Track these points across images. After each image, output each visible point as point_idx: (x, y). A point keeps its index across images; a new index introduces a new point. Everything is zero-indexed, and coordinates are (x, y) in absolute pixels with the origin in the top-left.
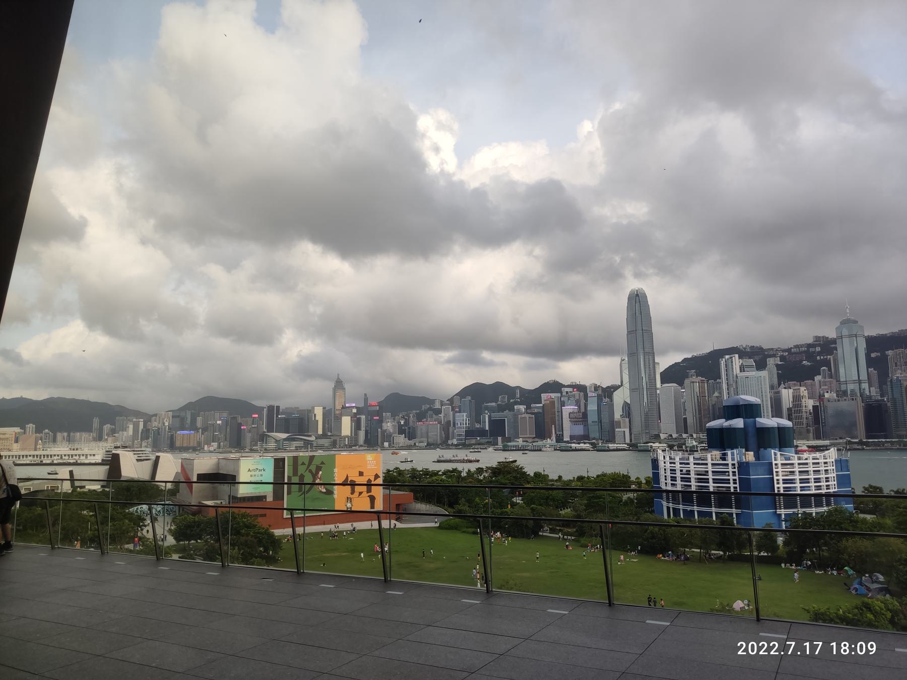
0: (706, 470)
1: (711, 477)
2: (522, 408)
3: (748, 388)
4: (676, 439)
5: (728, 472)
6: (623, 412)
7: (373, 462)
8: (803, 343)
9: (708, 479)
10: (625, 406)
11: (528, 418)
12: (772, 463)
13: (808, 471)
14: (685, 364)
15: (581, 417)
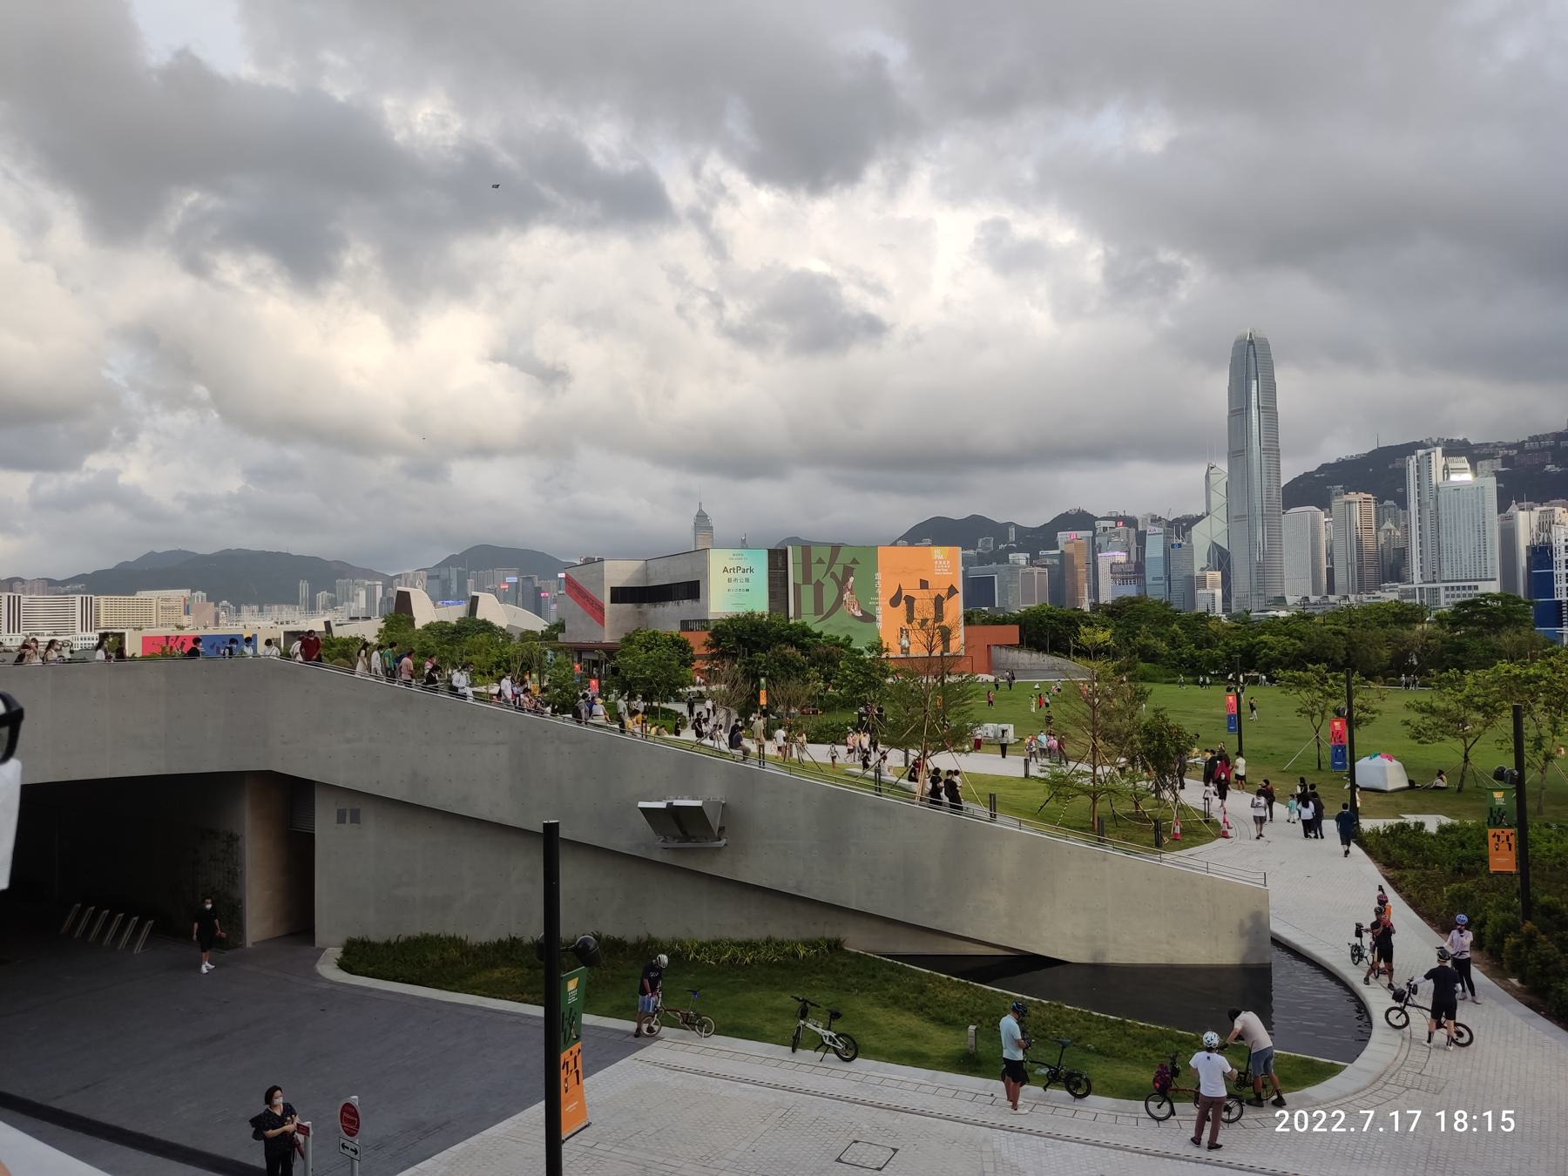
2: (1021, 558)
4: (1315, 604)
6: (1209, 561)
10: (1214, 553)
11: (1036, 575)
14: (1323, 475)
15: (1133, 570)
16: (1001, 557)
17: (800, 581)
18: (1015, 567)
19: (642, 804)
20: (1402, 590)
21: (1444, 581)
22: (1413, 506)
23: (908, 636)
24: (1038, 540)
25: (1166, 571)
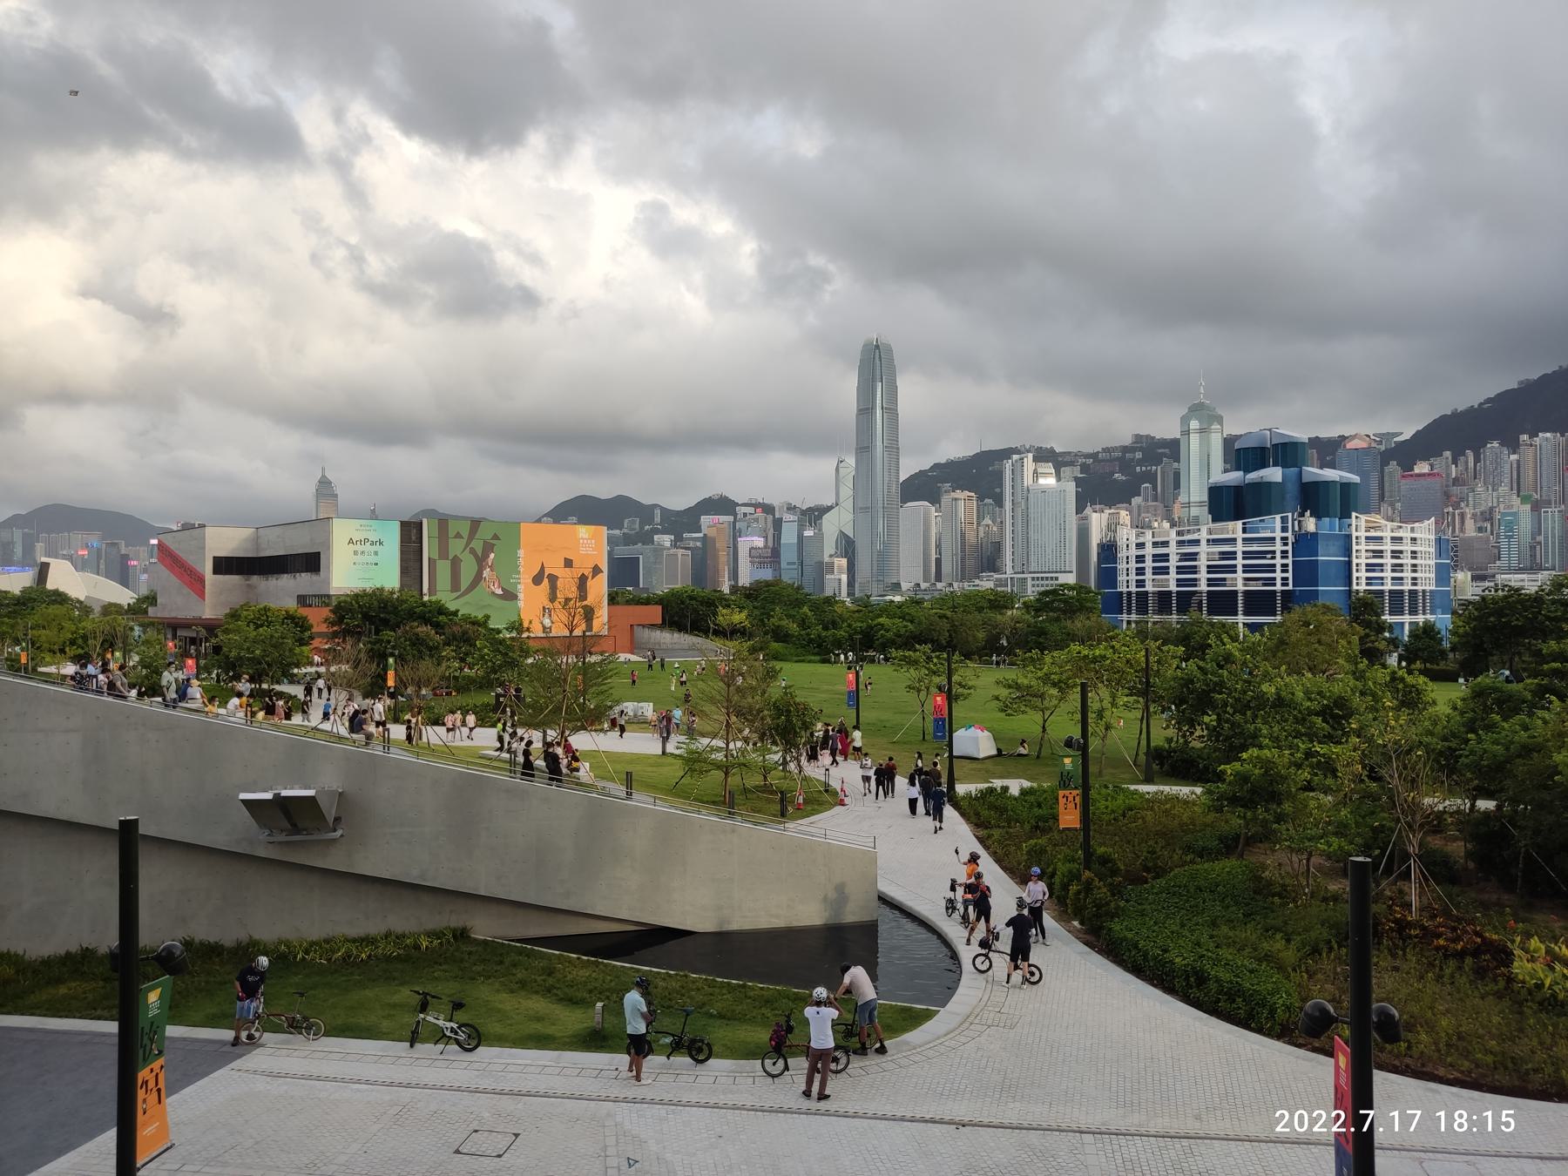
1: (1240, 562)
2: (666, 540)
3: (1045, 509)
4: (925, 590)
5: (1274, 552)
6: (837, 548)
7: (589, 541)
8: (1113, 446)
9: (1235, 566)
11: (680, 556)
12: (1351, 535)
16: (647, 538)
17: (437, 557)
18: (659, 550)
19: (244, 796)
20: (997, 580)
21: (1031, 573)
22: (1008, 505)
23: (550, 615)
24: (683, 522)
25: (799, 559)
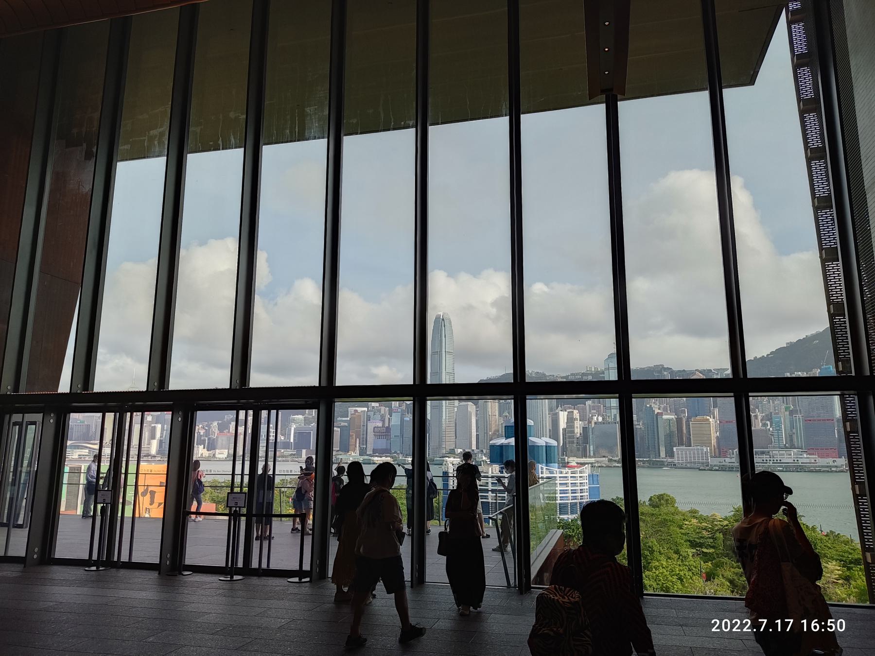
0: (487, 481)
13: (566, 484)
